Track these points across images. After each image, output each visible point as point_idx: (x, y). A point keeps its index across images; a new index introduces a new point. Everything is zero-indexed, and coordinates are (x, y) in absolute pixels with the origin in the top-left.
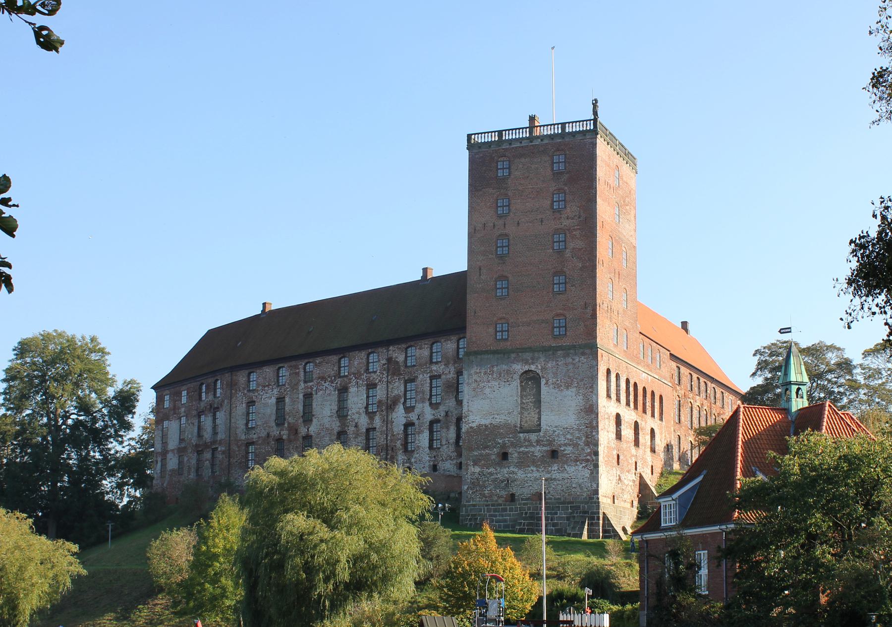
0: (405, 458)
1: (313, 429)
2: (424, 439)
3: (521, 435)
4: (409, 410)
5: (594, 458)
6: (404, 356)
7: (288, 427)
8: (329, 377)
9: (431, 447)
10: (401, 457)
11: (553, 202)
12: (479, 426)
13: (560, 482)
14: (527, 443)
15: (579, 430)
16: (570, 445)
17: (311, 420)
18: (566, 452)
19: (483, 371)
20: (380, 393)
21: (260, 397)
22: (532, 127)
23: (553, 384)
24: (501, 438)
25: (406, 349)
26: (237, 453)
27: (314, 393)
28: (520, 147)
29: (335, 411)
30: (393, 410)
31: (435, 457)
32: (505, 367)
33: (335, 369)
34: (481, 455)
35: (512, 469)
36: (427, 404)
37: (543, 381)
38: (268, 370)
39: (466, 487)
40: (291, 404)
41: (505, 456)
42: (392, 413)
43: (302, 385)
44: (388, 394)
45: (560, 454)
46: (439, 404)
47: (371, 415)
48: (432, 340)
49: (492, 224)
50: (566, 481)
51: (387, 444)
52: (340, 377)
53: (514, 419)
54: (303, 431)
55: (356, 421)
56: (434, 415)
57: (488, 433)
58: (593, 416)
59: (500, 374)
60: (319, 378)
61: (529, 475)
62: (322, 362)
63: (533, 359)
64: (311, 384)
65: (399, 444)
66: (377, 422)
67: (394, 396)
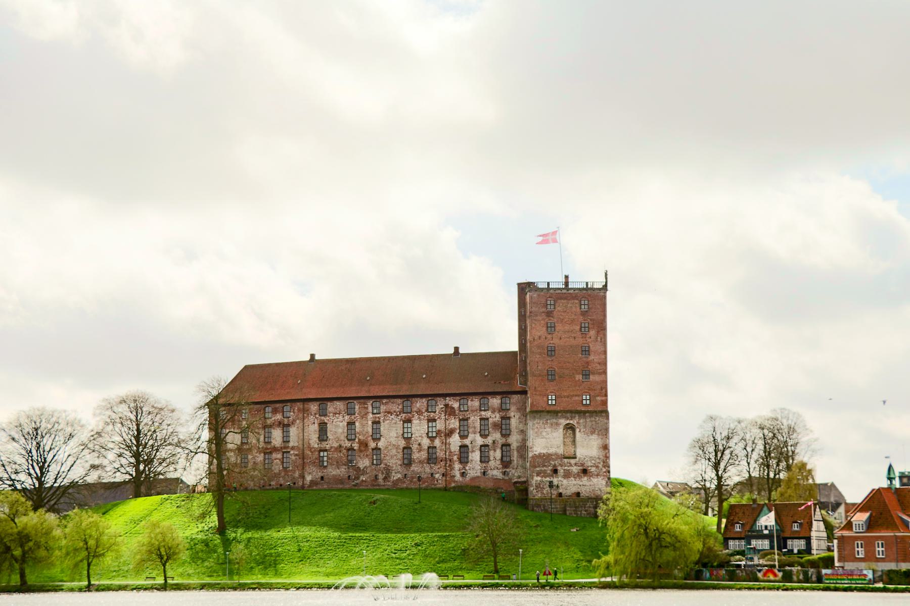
1: (381, 444)
2: (475, 456)
3: (565, 460)
4: (463, 437)
6: (458, 404)
8: (395, 412)
9: (481, 461)
10: (457, 466)
11: (581, 327)
14: (569, 465)
16: (594, 466)
17: (379, 439)
18: (591, 470)
19: (541, 422)
20: (440, 425)
22: (567, 283)
24: (553, 461)
25: (460, 400)
26: (311, 456)
28: (560, 293)
29: (400, 434)
31: (485, 467)
32: (554, 420)
33: (400, 407)
34: (541, 470)
35: (560, 479)
36: (478, 435)
37: (577, 430)
39: (532, 489)
40: (361, 427)
41: (555, 471)
43: (371, 415)
44: (446, 427)
45: (588, 472)
46: (488, 435)
47: (432, 439)
48: (481, 397)
49: (544, 337)
52: (404, 413)
53: (560, 451)
54: (372, 445)
55: (419, 442)
57: (545, 458)
58: (607, 451)
59: (552, 424)
61: (570, 482)
63: (571, 417)
64: (379, 415)
65: (455, 458)
66: (437, 443)
67: (451, 429)
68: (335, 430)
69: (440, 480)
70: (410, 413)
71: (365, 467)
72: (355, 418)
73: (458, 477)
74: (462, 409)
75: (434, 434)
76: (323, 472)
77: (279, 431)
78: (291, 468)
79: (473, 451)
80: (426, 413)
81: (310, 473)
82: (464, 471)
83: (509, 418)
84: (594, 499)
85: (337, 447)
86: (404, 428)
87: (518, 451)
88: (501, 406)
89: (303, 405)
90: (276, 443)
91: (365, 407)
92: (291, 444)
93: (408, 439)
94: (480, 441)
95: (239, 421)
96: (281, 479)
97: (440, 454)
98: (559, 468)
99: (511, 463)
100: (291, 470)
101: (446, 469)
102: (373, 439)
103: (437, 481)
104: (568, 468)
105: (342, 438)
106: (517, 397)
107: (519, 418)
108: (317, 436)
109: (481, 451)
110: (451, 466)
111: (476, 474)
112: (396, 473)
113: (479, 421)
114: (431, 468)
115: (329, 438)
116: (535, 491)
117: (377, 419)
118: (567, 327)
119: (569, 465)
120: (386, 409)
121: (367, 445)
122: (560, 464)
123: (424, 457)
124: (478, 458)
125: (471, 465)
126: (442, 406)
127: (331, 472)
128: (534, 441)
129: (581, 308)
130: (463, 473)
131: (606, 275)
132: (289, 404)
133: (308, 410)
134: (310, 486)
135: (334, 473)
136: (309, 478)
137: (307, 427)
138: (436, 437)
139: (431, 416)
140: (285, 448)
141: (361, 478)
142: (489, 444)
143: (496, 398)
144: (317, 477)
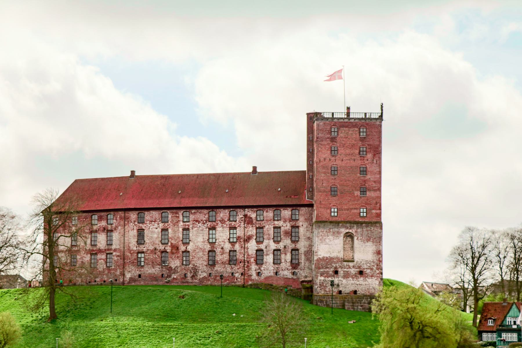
0: (257, 267)
1: (190, 248)
2: (269, 259)
4: (259, 242)
5: (381, 275)
6: (255, 215)
7: (171, 245)
8: (202, 221)
9: (274, 263)
10: (254, 267)
11: (360, 151)
12: (324, 257)
13: (364, 286)
14: (348, 267)
15: (373, 262)
16: (369, 269)
17: (188, 243)
18: (367, 272)
19: (325, 231)
20: (239, 232)
21: (148, 227)
22: (348, 114)
23: (361, 239)
24: (335, 264)
25: (257, 211)
26: (130, 257)
27: (190, 228)
28: (343, 122)
29: (206, 240)
30: (249, 242)
31: (277, 268)
32: (336, 230)
34: (324, 271)
35: (340, 279)
36: (272, 241)
37: (355, 238)
38: (154, 213)
39: (317, 287)
40: (173, 233)
41: (336, 272)
42: (247, 243)
43: (181, 223)
44: (245, 233)
45: (364, 273)
46: (280, 241)
47: (233, 244)
48: (275, 208)
49: (329, 159)
50: (367, 286)
51: (244, 259)
52: (209, 221)
53: (341, 255)
54: (182, 248)
55: (222, 246)
56: (276, 247)
57: (328, 261)
58: (380, 256)
59: (334, 233)
60: (194, 221)
61: (349, 282)
62: (196, 212)
63: (350, 227)
64: (188, 223)
65: (252, 260)
67: (249, 235)
68: (151, 236)
69: (239, 278)
70: (215, 222)
71: (176, 267)
72: (168, 225)
73: (254, 276)
74: (259, 219)
75: (235, 240)
76: (140, 271)
77: (103, 235)
78: (113, 267)
79: (267, 255)
80: (228, 222)
81: (129, 272)
82: (259, 271)
83: (298, 227)
84: (369, 296)
85: (153, 250)
86: (209, 234)
87: (305, 255)
88: (292, 216)
89: (125, 213)
90: (101, 246)
91: (176, 217)
92: (113, 247)
93: (212, 244)
94: (273, 246)
95: (70, 227)
96: (105, 276)
97: (240, 257)
98: (339, 270)
99: (299, 265)
100: (114, 269)
101: (244, 269)
102: (183, 243)
103: (237, 280)
104: (348, 270)
105: (158, 241)
106: (305, 209)
107: (307, 227)
108: (136, 240)
109: (274, 255)
110: (249, 267)
111: (269, 274)
112: (202, 272)
113: (272, 229)
114: (232, 268)
115: (146, 242)
116: (319, 289)
117: (187, 227)
118: (348, 151)
119: (348, 267)
120: (194, 218)
121: (178, 248)
122: (340, 267)
123: (226, 259)
124: (272, 261)
125: (265, 267)
126: (242, 216)
127: (148, 271)
128: (319, 246)
129: (360, 135)
130: (259, 273)
131: (382, 107)
132: (112, 213)
133: (128, 218)
134: (129, 283)
135: (150, 271)
136: (128, 276)
137: (127, 232)
138: (236, 242)
139: (233, 224)
140: (108, 250)
141: (172, 277)
142: (281, 249)
143: (287, 210)
144: (135, 275)
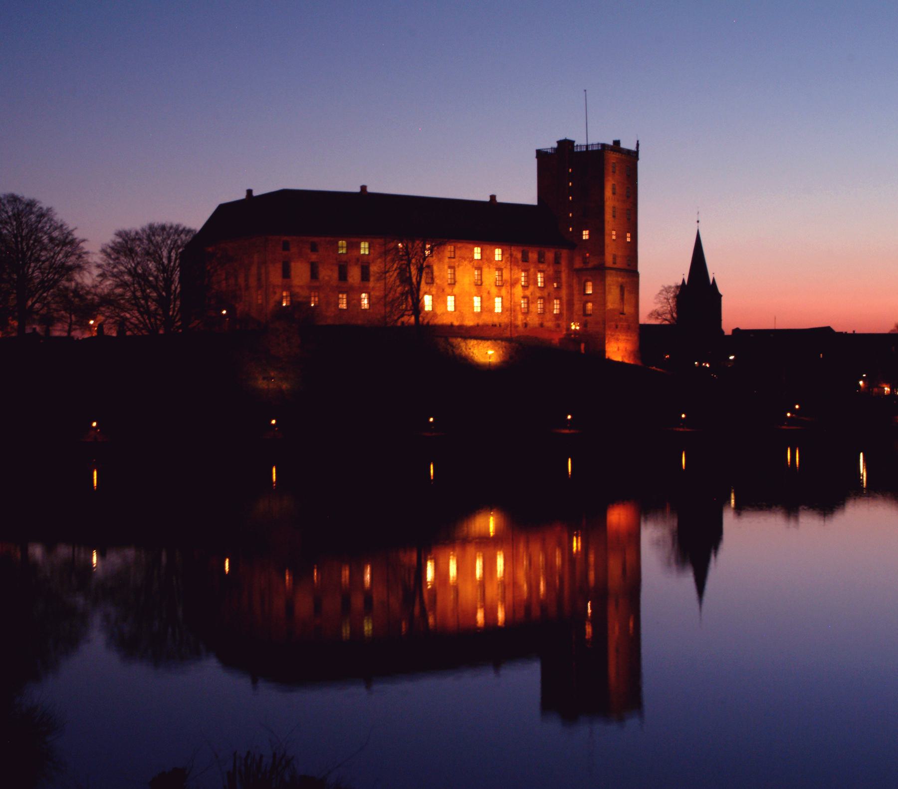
27: (456, 267)
56: (541, 294)
